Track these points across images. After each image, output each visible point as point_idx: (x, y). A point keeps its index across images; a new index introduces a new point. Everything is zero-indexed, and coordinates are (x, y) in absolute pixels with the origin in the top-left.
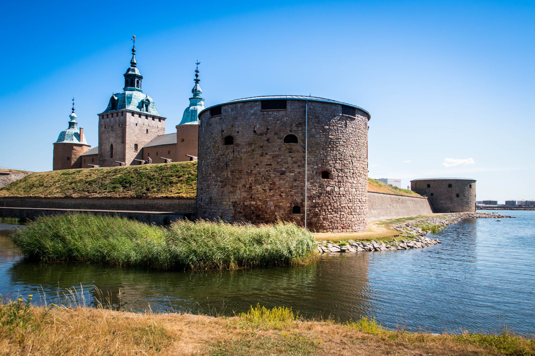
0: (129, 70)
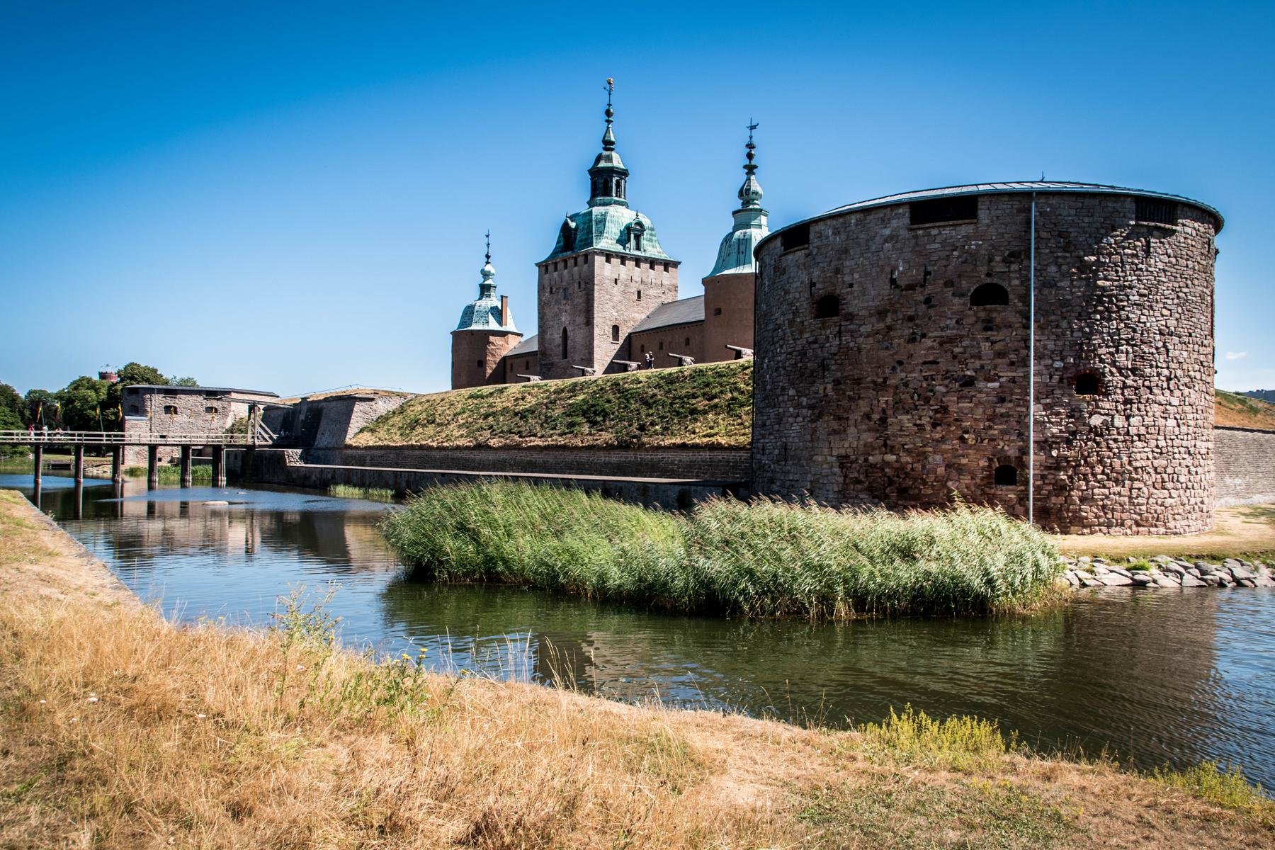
0: (599, 158)
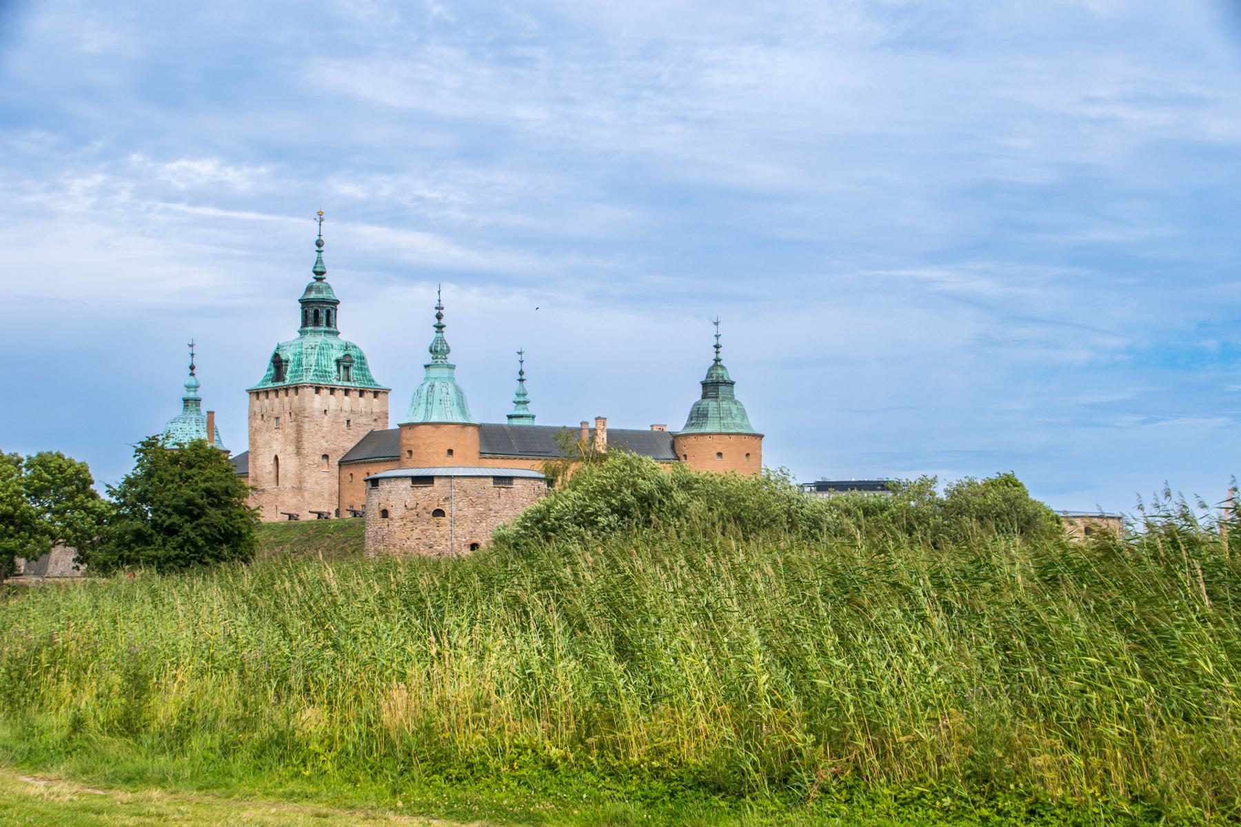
0: (309, 289)
